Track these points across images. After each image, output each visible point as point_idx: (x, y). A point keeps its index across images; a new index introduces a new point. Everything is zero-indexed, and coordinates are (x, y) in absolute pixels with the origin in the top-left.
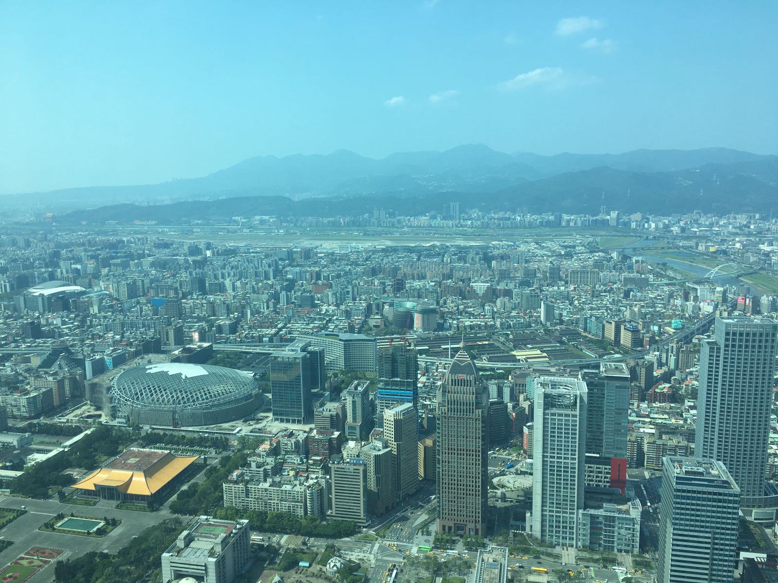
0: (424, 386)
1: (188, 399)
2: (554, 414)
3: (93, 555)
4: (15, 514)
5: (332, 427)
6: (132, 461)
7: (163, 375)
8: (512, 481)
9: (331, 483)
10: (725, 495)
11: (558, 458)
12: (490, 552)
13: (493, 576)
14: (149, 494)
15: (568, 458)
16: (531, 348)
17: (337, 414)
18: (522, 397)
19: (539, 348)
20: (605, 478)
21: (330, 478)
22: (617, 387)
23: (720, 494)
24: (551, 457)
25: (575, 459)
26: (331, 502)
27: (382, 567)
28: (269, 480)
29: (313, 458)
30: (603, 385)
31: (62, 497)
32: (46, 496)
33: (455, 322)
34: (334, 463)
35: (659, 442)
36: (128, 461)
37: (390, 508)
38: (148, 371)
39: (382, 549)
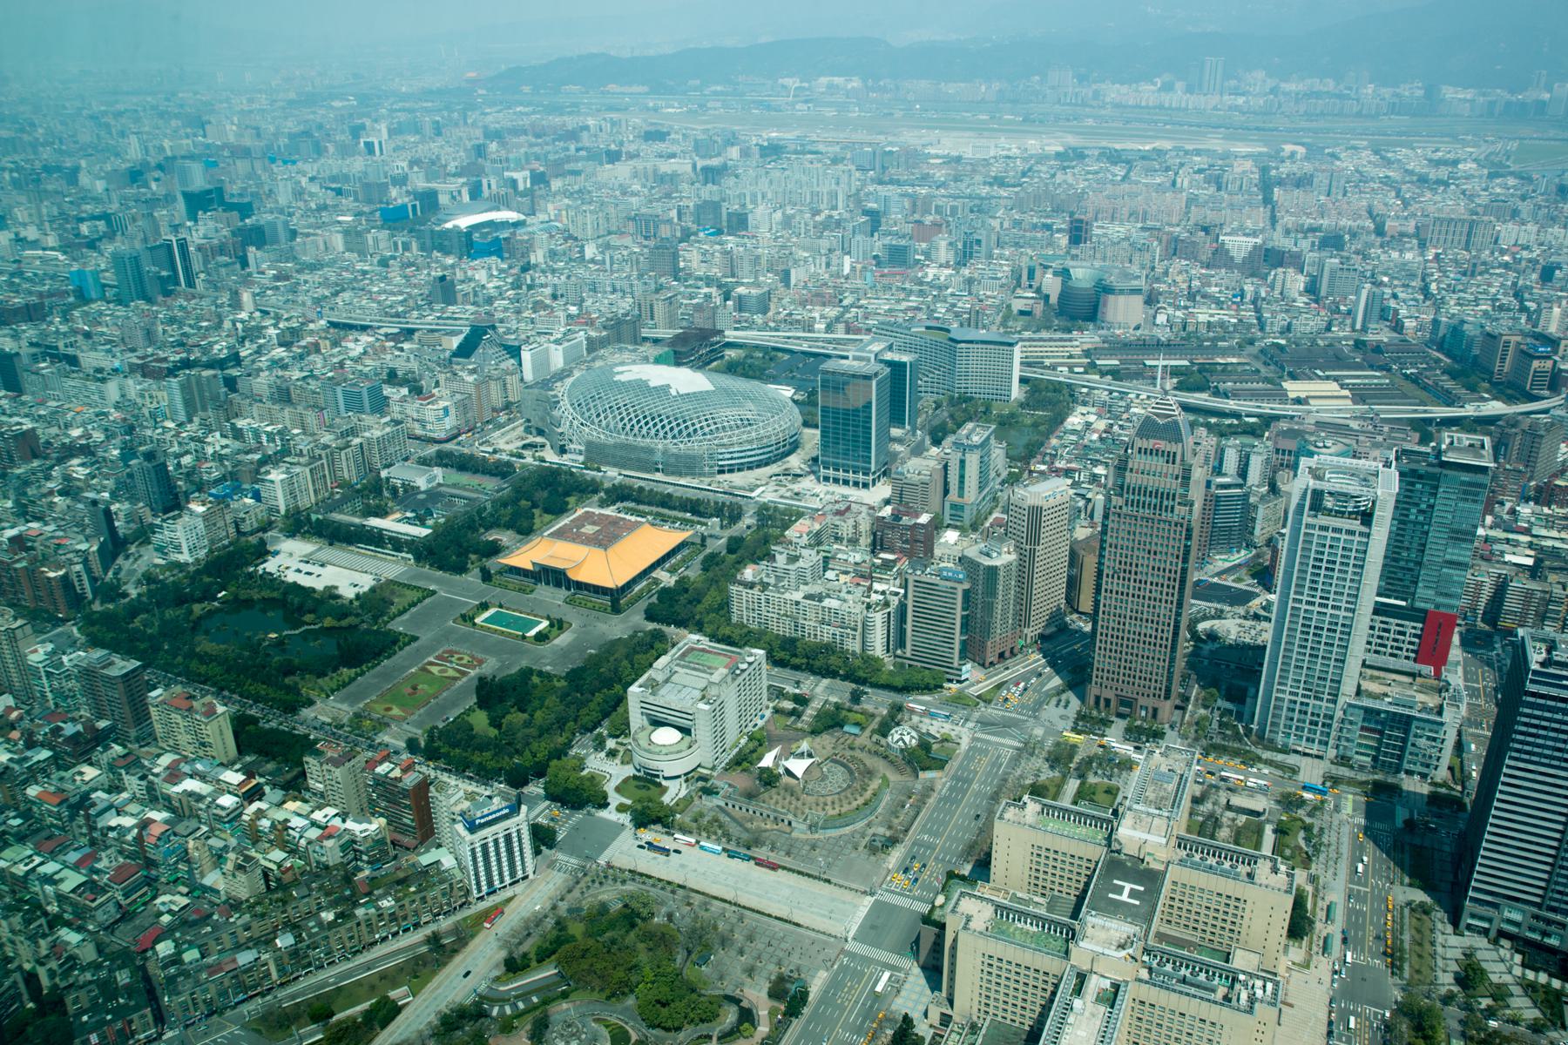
1: (680, 432)
2: (1322, 528)
3: (527, 673)
4: (420, 594)
6: (589, 529)
7: (641, 386)
11: (1320, 605)
13: (1162, 793)
14: (610, 584)
15: (1339, 608)
16: (1320, 378)
19: (1336, 379)
20: (1411, 643)
22: (1463, 483)
24: (1308, 603)
27: (981, 751)
29: (882, 555)
31: (486, 576)
32: (461, 569)
33: (1179, 313)
37: (1007, 654)
38: (617, 378)
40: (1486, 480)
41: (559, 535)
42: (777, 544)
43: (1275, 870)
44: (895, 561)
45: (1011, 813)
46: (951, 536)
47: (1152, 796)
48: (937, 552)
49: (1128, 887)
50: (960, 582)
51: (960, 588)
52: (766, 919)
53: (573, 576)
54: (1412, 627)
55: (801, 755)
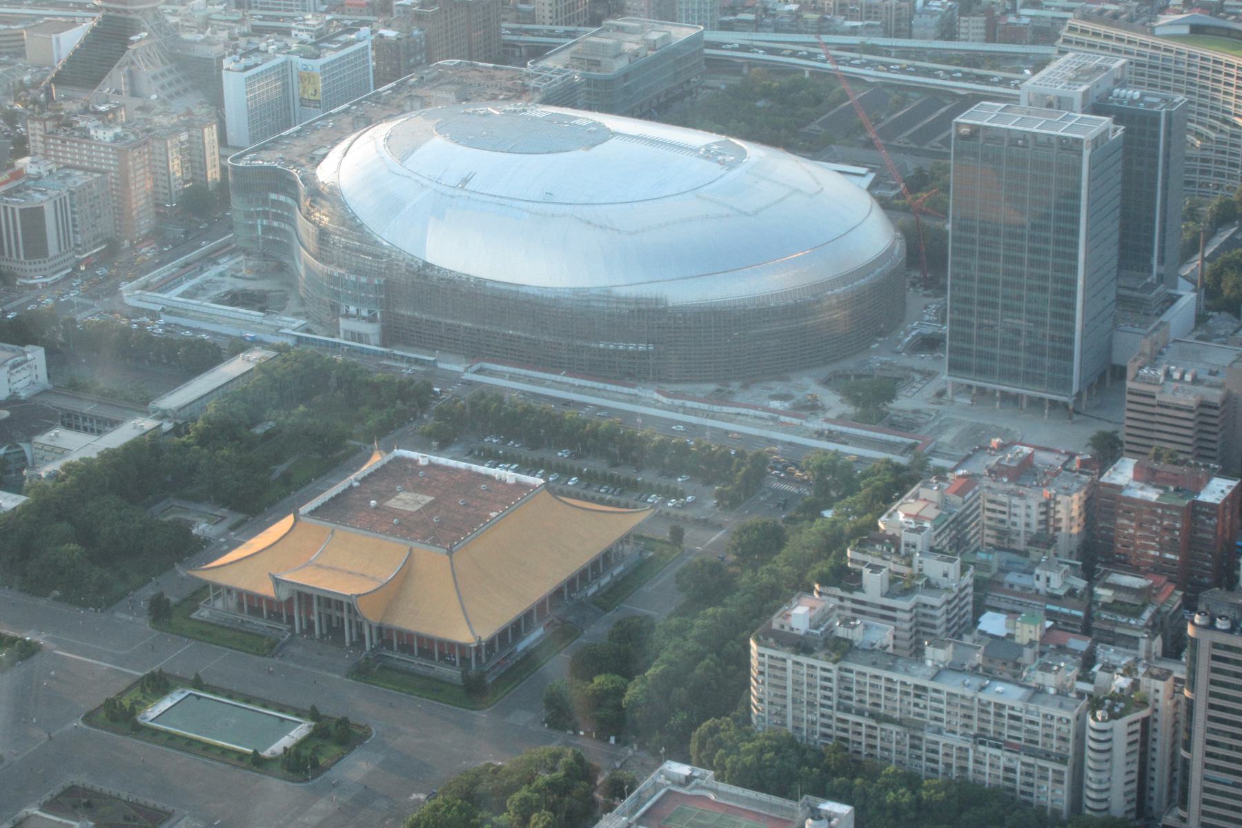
5: (1202, 453)
6: (407, 501)
9: (1190, 704)
14: (463, 635)
26: (1186, 777)
28: (935, 655)
31: (160, 611)
32: (104, 598)
34: (1211, 626)
36: (393, 503)
41: (334, 510)
42: (861, 546)
53: (371, 614)
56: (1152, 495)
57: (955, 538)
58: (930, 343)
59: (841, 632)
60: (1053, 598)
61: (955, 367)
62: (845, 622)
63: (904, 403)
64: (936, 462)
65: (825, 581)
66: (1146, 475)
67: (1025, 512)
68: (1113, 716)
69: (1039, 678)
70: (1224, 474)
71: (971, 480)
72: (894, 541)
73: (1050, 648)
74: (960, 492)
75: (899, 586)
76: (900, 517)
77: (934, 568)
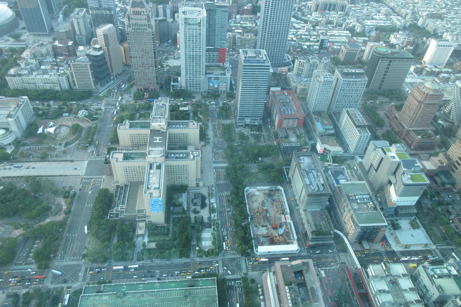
0: (121, 9)
8: (172, 63)
10: (264, 66)
12: (160, 101)
15: (197, 52)
17: (69, 30)
18: (176, 15)
21: (71, 70)
22: (222, 11)
23: (262, 66)
24: (189, 51)
25: (200, 52)
28: (34, 73)
30: (215, 10)
34: (71, 62)
35: (243, 37)
39: (107, 104)
40: (227, 9)
42: (19, 60)
43: (194, 124)
44: (64, 59)
45: (121, 127)
46: (81, 48)
47: (159, 113)
48: (78, 53)
49: (158, 138)
50: (87, 62)
51: (88, 64)
52: (55, 177)
54: (216, 54)
55: (51, 127)
56: (61, 45)
57: (34, 56)
58: (24, 28)
59: (19, 73)
60: (51, 62)
61: (28, 31)
62: (20, 71)
63: (22, 38)
64: (30, 46)
65: (15, 66)
66: (60, 43)
67: (44, 50)
68: (62, 76)
69: (51, 73)
70: (71, 40)
71: (34, 47)
72: (24, 58)
73: (52, 69)
74: (33, 50)
75: (27, 64)
76: (24, 55)
77: (31, 61)
